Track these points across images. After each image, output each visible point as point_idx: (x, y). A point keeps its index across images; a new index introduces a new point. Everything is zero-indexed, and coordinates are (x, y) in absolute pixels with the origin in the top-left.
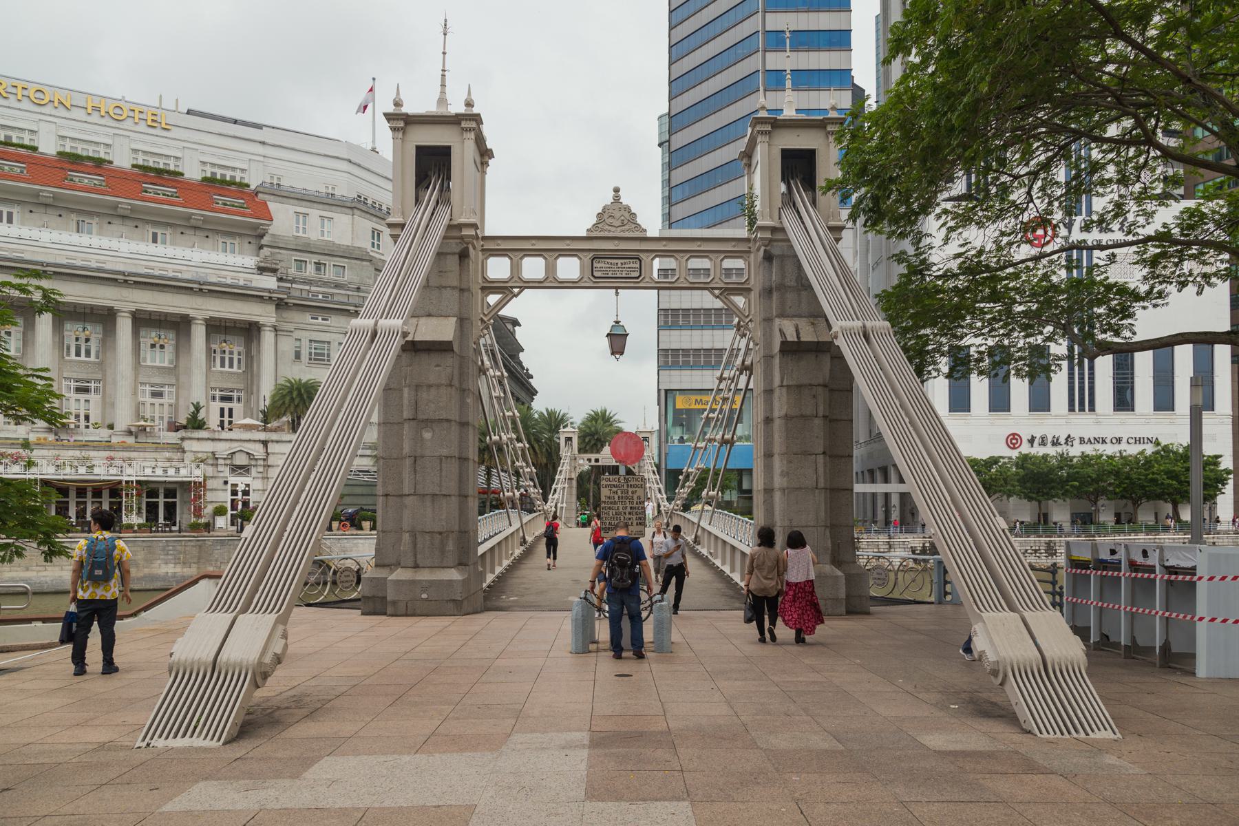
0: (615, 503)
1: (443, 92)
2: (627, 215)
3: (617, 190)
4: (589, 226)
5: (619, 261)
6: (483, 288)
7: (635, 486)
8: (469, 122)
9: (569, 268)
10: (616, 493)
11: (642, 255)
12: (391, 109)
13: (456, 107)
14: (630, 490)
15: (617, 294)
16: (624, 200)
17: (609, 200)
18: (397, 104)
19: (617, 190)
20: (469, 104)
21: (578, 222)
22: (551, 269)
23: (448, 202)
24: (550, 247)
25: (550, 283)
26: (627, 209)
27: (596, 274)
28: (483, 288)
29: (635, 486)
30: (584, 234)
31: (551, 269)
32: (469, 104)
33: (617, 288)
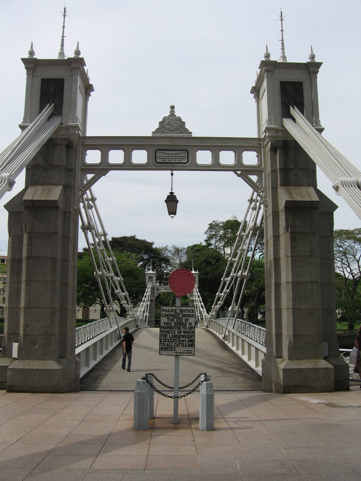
0: (172, 328)
1: (62, 49)
2: (179, 124)
3: (172, 107)
4: (154, 130)
5: (174, 152)
6: (82, 170)
7: (188, 316)
8: (77, 64)
9: (140, 156)
10: (172, 320)
11: (189, 149)
12: (27, 56)
13: (69, 54)
14: (184, 318)
15: (172, 174)
16: (177, 114)
17: (167, 114)
18: (32, 53)
19: (172, 107)
20: (78, 52)
21: (147, 128)
22: (128, 157)
23: (61, 114)
24: (128, 144)
25: (128, 165)
26: (179, 119)
27: (158, 161)
28: (82, 170)
29: (188, 316)
30: (150, 135)
31: (128, 157)
32: (78, 52)
33: (172, 170)
